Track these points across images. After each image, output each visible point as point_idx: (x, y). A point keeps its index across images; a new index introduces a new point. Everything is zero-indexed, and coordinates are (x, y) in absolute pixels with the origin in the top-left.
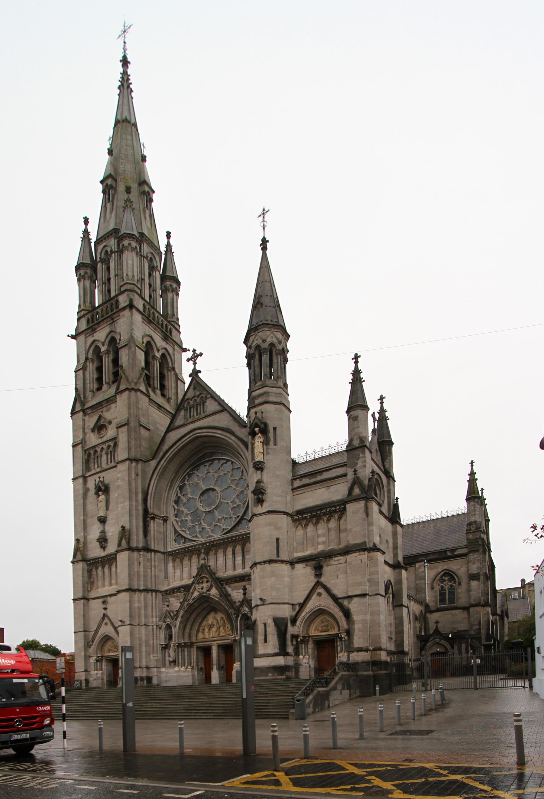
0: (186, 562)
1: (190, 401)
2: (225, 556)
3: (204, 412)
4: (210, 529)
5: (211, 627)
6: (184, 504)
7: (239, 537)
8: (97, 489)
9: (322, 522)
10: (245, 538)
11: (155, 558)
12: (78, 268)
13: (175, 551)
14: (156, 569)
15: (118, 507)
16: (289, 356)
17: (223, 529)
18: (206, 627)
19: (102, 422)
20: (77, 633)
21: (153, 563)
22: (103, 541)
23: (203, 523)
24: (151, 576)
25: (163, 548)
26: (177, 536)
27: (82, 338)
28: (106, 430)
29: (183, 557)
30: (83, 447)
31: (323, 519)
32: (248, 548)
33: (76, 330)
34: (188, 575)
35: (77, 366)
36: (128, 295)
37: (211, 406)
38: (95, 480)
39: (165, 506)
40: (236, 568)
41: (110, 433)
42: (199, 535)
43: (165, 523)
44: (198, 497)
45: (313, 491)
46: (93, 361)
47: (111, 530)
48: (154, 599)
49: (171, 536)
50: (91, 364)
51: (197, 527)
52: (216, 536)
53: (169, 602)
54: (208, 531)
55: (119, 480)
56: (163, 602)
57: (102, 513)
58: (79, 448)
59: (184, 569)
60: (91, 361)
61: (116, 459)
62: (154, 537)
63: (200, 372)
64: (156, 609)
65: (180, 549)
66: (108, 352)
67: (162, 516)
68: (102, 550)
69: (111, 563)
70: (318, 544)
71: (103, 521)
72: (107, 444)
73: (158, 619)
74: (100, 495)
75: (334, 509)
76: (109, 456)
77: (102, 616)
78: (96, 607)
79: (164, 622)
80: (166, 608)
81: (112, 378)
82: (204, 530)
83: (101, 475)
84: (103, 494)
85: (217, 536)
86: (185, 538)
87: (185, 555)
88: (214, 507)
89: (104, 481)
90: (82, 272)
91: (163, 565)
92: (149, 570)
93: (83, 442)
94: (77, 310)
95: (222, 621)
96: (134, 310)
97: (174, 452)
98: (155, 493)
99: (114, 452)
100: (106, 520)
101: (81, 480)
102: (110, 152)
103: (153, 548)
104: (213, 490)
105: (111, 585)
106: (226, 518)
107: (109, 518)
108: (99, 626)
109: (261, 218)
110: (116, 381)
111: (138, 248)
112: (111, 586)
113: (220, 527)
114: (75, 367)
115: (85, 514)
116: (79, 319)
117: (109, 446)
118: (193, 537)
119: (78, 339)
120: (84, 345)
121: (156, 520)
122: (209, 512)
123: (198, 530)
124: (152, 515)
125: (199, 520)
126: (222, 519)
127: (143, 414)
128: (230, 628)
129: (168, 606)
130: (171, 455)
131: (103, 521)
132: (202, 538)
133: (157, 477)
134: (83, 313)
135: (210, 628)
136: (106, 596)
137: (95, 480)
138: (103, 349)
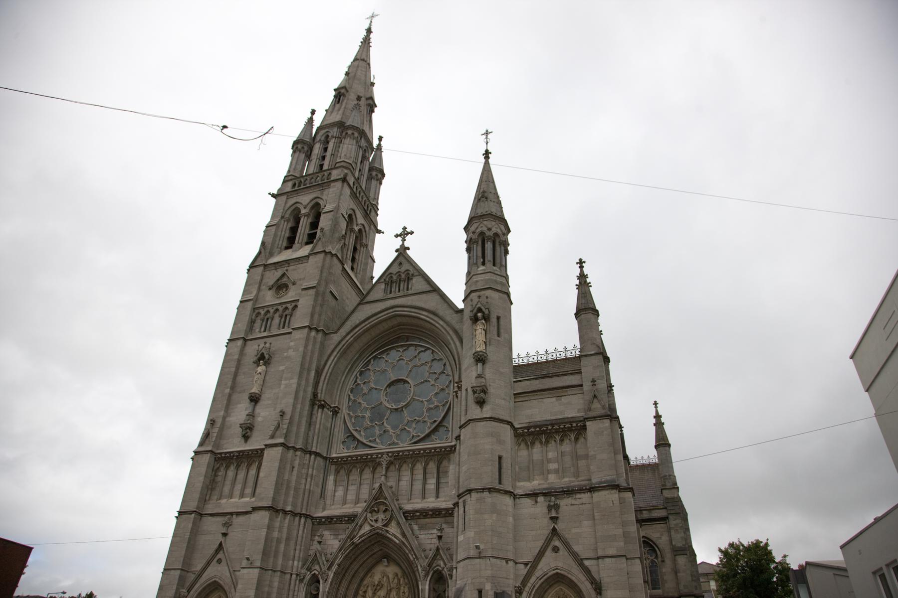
0: (355, 476)
1: (393, 276)
2: (412, 475)
3: (408, 289)
4: (394, 433)
5: (379, 586)
6: (365, 394)
7: (435, 450)
8: (258, 356)
9: (553, 442)
10: (442, 453)
11: (314, 463)
12: (296, 143)
13: (342, 458)
14: (313, 481)
15: (280, 384)
16: (509, 248)
17: (413, 436)
18: (370, 588)
19: (285, 280)
20: (168, 572)
21: (310, 470)
22: (247, 431)
23: (385, 424)
24: (305, 490)
25: (326, 450)
26: (348, 437)
27: (284, 198)
28: (287, 290)
29: (351, 468)
30: (254, 304)
31: (555, 438)
32: (445, 467)
33: (279, 190)
34: (354, 498)
35: (269, 222)
36: (342, 170)
37: (417, 284)
38: (259, 345)
39: (339, 394)
40: (426, 495)
41: (291, 295)
42: (377, 440)
43: (334, 416)
44: (383, 389)
45: (540, 400)
46: (288, 221)
47: (262, 414)
48: (301, 528)
49: (339, 434)
50: (286, 223)
51: (377, 428)
52: (402, 445)
53: (321, 536)
54: (391, 436)
55: (290, 350)
56: (311, 535)
57: (255, 390)
58: (250, 303)
59: (350, 488)
60: (287, 220)
61: (291, 325)
62: (319, 433)
63: (408, 249)
64: (301, 546)
65: (349, 456)
66: (307, 215)
67: (332, 406)
68: (243, 440)
69: (250, 462)
70: (549, 472)
71: (255, 399)
72: (284, 306)
73: (300, 563)
74: (261, 364)
75: (570, 426)
76: (283, 320)
77: (216, 546)
78: (212, 527)
79: (309, 569)
80: (316, 546)
81: (305, 239)
82: (387, 433)
83: (268, 340)
84: (263, 365)
85: (404, 446)
86: (359, 441)
87: (355, 467)
88: (404, 404)
89: (270, 348)
90: (299, 146)
91: (322, 476)
92: (303, 481)
93: (256, 299)
94: (285, 174)
95: (396, 581)
96: (345, 184)
97: (365, 328)
98: (331, 373)
99: (291, 316)
100: (259, 399)
101: (240, 343)
102: (347, 74)
103: (314, 449)
104: (405, 382)
105: (242, 496)
106: (419, 421)
107: (263, 397)
108: (208, 564)
109: (484, 136)
110: (312, 242)
111: (359, 138)
112: (242, 498)
113: (409, 432)
114: (267, 223)
115: (233, 388)
116: (285, 182)
117: (286, 308)
118: (370, 441)
119: (278, 198)
120: (283, 205)
121: (325, 409)
122: (396, 410)
123: (378, 432)
124: (323, 402)
125: (381, 419)
126: (412, 421)
127: (335, 282)
128: (407, 594)
129: (320, 542)
130: (361, 331)
131: (255, 399)
132: (382, 445)
133: (338, 355)
134: (290, 178)
135: (375, 590)
136: (231, 514)
137: (259, 345)
138: (303, 211)
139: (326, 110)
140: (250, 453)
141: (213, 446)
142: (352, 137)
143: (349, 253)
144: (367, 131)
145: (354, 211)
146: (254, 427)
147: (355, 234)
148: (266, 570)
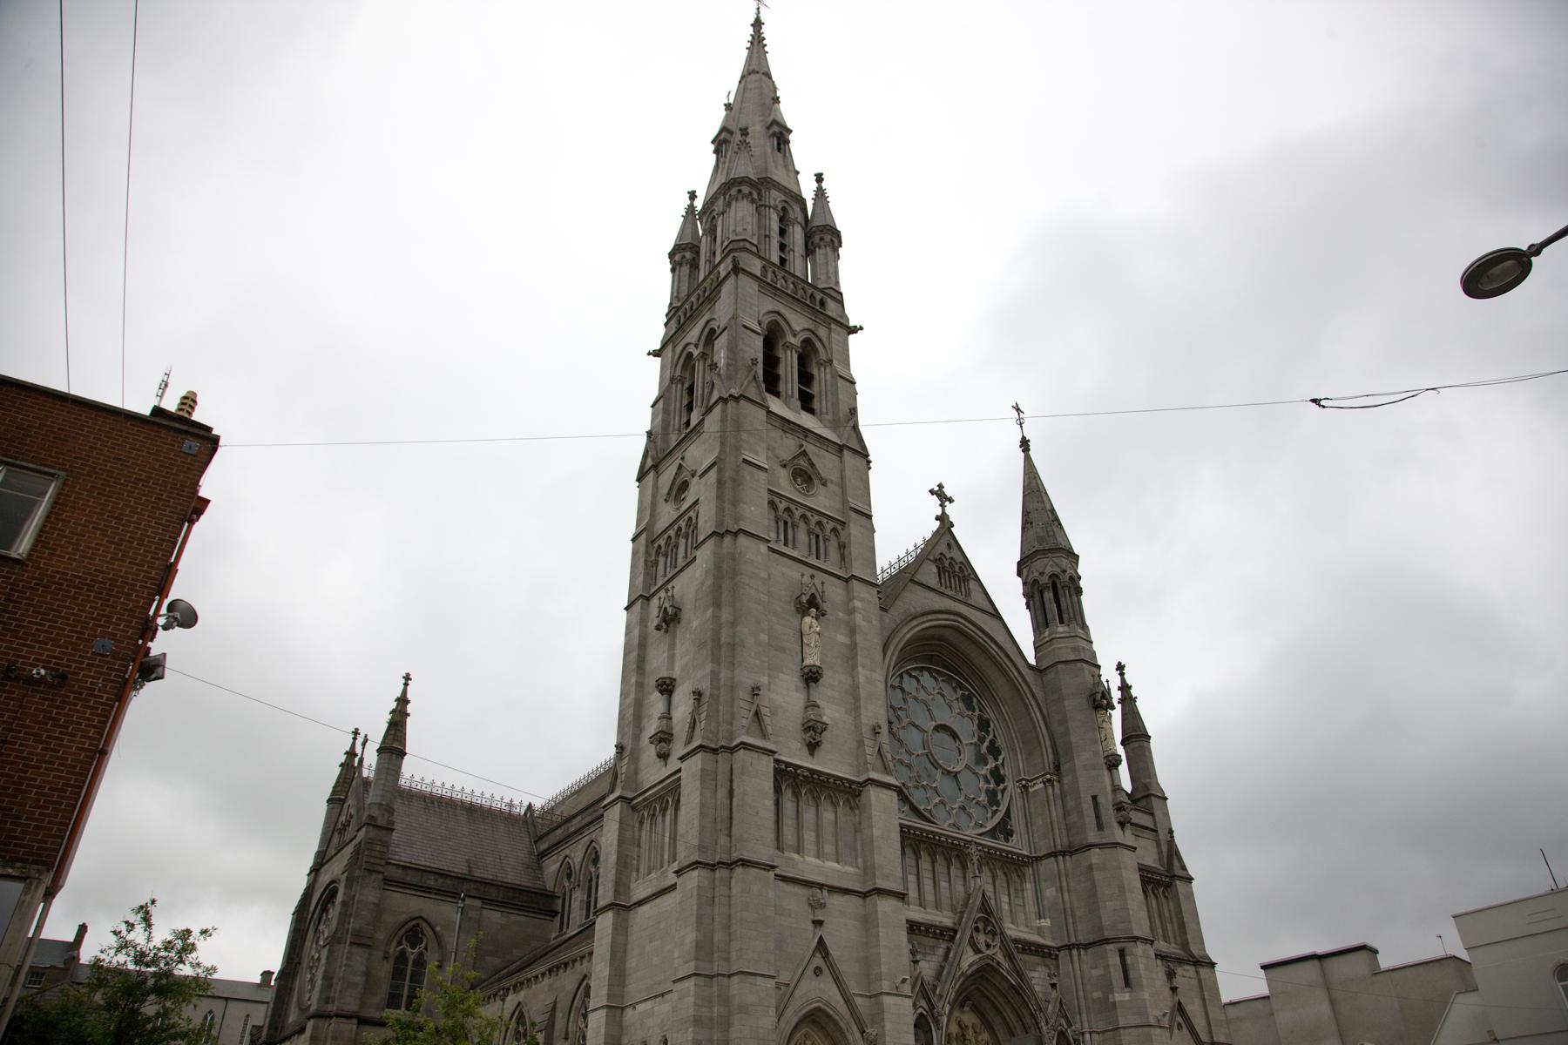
139: (798, 173)
140: (831, 780)
141: (623, 789)
142: (740, 196)
143: (700, 392)
144: (779, 176)
145: (778, 313)
146: (672, 735)
147: (794, 352)
148: (730, 976)
